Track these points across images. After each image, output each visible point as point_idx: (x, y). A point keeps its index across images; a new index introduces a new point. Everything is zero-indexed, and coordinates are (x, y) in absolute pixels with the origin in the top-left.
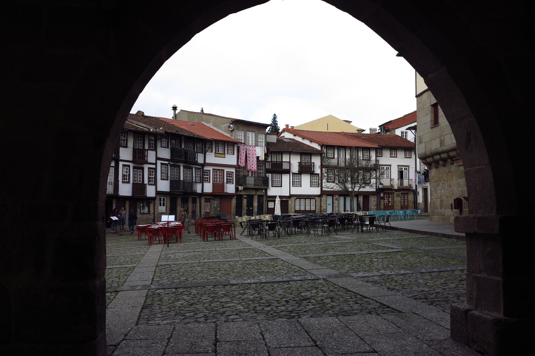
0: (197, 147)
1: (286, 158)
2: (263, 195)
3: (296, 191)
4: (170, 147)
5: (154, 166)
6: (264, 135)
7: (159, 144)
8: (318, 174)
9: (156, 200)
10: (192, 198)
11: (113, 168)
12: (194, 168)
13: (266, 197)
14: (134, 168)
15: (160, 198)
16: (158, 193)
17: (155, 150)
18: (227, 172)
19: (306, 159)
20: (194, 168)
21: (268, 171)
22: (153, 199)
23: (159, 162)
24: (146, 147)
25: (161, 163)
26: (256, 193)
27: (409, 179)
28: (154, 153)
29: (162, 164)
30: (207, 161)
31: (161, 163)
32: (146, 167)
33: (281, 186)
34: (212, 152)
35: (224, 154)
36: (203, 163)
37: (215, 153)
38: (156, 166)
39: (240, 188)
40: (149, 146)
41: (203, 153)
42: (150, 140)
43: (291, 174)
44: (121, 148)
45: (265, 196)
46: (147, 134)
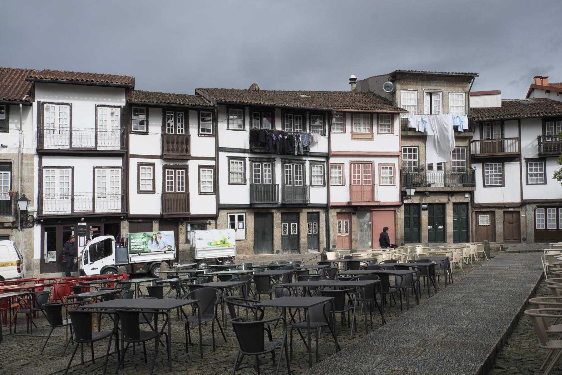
2: (467, 204)
5: (213, 163)
6: (464, 94)
10: (308, 213)
11: (120, 170)
13: (472, 207)
14: (165, 167)
15: (230, 216)
16: (220, 207)
21: (474, 159)
23: (223, 157)
25: (227, 156)
26: (449, 200)
28: (213, 139)
29: (230, 158)
30: (334, 149)
31: (227, 156)
32: (193, 165)
35: (372, 133)
36: (327, 152)
37: (352, 133)
38: (217, 162)
43: (523, 161)
44: (130, 135)
45: (470, 204)
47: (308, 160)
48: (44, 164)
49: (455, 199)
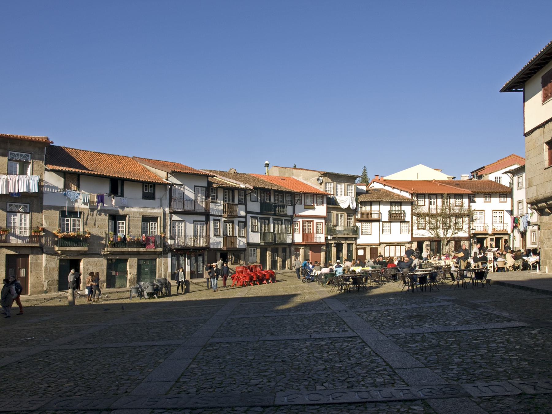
0: (286, 200)
1: (375, 208)
3: (386, 238)
4: (259, 201)
5: (244, 220)
7: (248, 198)
8: (408, 222)
9: (246, 251)
12: (283, 220)
16: (248, 244)
17: (245, 204)
18: (316, 222)
19: (396, 208)
20: (283, 220)
22: (244, 250)
24: (236, 201)
27: (504, 223)
28: (244, 207)
33: (371, 235)
34: (301, 204)
37: (305, 205)
38: (246, 220)
39: (330, 237)
40: (239, 201)
41: (292, 205)
42: (239, 195)
46: (236, 190)
47: (284, 219)
48: (173, 219)
49: (348, 242)
